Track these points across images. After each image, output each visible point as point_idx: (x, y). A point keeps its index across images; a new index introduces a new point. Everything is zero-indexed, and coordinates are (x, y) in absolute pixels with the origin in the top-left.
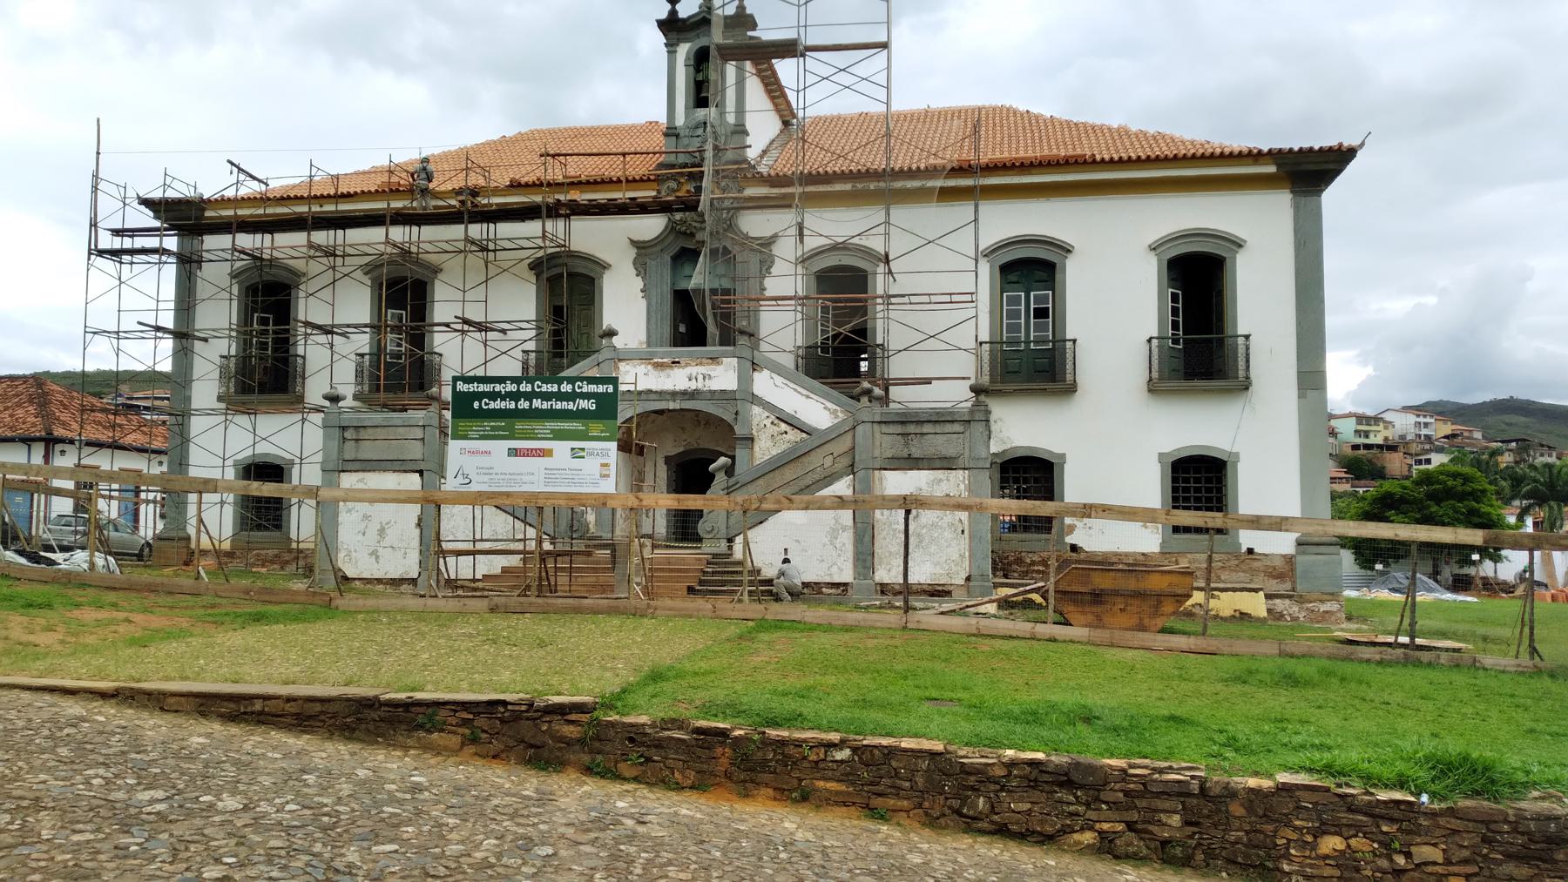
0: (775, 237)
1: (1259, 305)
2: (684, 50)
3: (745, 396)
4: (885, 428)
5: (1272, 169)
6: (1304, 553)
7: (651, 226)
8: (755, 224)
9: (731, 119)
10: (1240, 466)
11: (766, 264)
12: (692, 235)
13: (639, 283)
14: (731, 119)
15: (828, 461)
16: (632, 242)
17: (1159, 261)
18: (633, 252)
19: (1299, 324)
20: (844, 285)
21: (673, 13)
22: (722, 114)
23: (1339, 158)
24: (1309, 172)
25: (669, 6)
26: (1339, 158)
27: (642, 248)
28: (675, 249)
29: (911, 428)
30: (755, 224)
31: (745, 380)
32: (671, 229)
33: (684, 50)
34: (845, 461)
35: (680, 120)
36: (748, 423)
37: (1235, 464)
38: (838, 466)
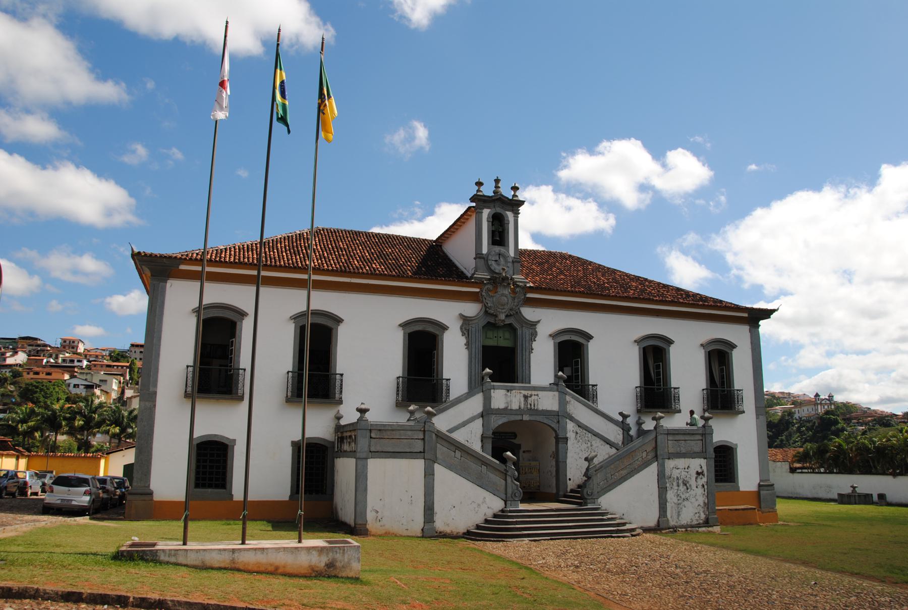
0: (539, 322)
3: (561, 415)
4: (670, 438)
5: (746, 315)
8: (529, 313)
9: (512, 253)
10: (738, 450)
11: (534, 335)
12: (496, 316)
13: (463, 340)
14: (512, 253)
15: (644, 454)
18: (460, 323)
20: (571, 352)
21: (478, 191)
23: (767, 314)
26: (767, 314)
27: (466, 322)
28: (485, 322)
29: (681, 437)
30: (529, 313)
31: (563, 403)
33: (486, 213)
38: (649, 457)
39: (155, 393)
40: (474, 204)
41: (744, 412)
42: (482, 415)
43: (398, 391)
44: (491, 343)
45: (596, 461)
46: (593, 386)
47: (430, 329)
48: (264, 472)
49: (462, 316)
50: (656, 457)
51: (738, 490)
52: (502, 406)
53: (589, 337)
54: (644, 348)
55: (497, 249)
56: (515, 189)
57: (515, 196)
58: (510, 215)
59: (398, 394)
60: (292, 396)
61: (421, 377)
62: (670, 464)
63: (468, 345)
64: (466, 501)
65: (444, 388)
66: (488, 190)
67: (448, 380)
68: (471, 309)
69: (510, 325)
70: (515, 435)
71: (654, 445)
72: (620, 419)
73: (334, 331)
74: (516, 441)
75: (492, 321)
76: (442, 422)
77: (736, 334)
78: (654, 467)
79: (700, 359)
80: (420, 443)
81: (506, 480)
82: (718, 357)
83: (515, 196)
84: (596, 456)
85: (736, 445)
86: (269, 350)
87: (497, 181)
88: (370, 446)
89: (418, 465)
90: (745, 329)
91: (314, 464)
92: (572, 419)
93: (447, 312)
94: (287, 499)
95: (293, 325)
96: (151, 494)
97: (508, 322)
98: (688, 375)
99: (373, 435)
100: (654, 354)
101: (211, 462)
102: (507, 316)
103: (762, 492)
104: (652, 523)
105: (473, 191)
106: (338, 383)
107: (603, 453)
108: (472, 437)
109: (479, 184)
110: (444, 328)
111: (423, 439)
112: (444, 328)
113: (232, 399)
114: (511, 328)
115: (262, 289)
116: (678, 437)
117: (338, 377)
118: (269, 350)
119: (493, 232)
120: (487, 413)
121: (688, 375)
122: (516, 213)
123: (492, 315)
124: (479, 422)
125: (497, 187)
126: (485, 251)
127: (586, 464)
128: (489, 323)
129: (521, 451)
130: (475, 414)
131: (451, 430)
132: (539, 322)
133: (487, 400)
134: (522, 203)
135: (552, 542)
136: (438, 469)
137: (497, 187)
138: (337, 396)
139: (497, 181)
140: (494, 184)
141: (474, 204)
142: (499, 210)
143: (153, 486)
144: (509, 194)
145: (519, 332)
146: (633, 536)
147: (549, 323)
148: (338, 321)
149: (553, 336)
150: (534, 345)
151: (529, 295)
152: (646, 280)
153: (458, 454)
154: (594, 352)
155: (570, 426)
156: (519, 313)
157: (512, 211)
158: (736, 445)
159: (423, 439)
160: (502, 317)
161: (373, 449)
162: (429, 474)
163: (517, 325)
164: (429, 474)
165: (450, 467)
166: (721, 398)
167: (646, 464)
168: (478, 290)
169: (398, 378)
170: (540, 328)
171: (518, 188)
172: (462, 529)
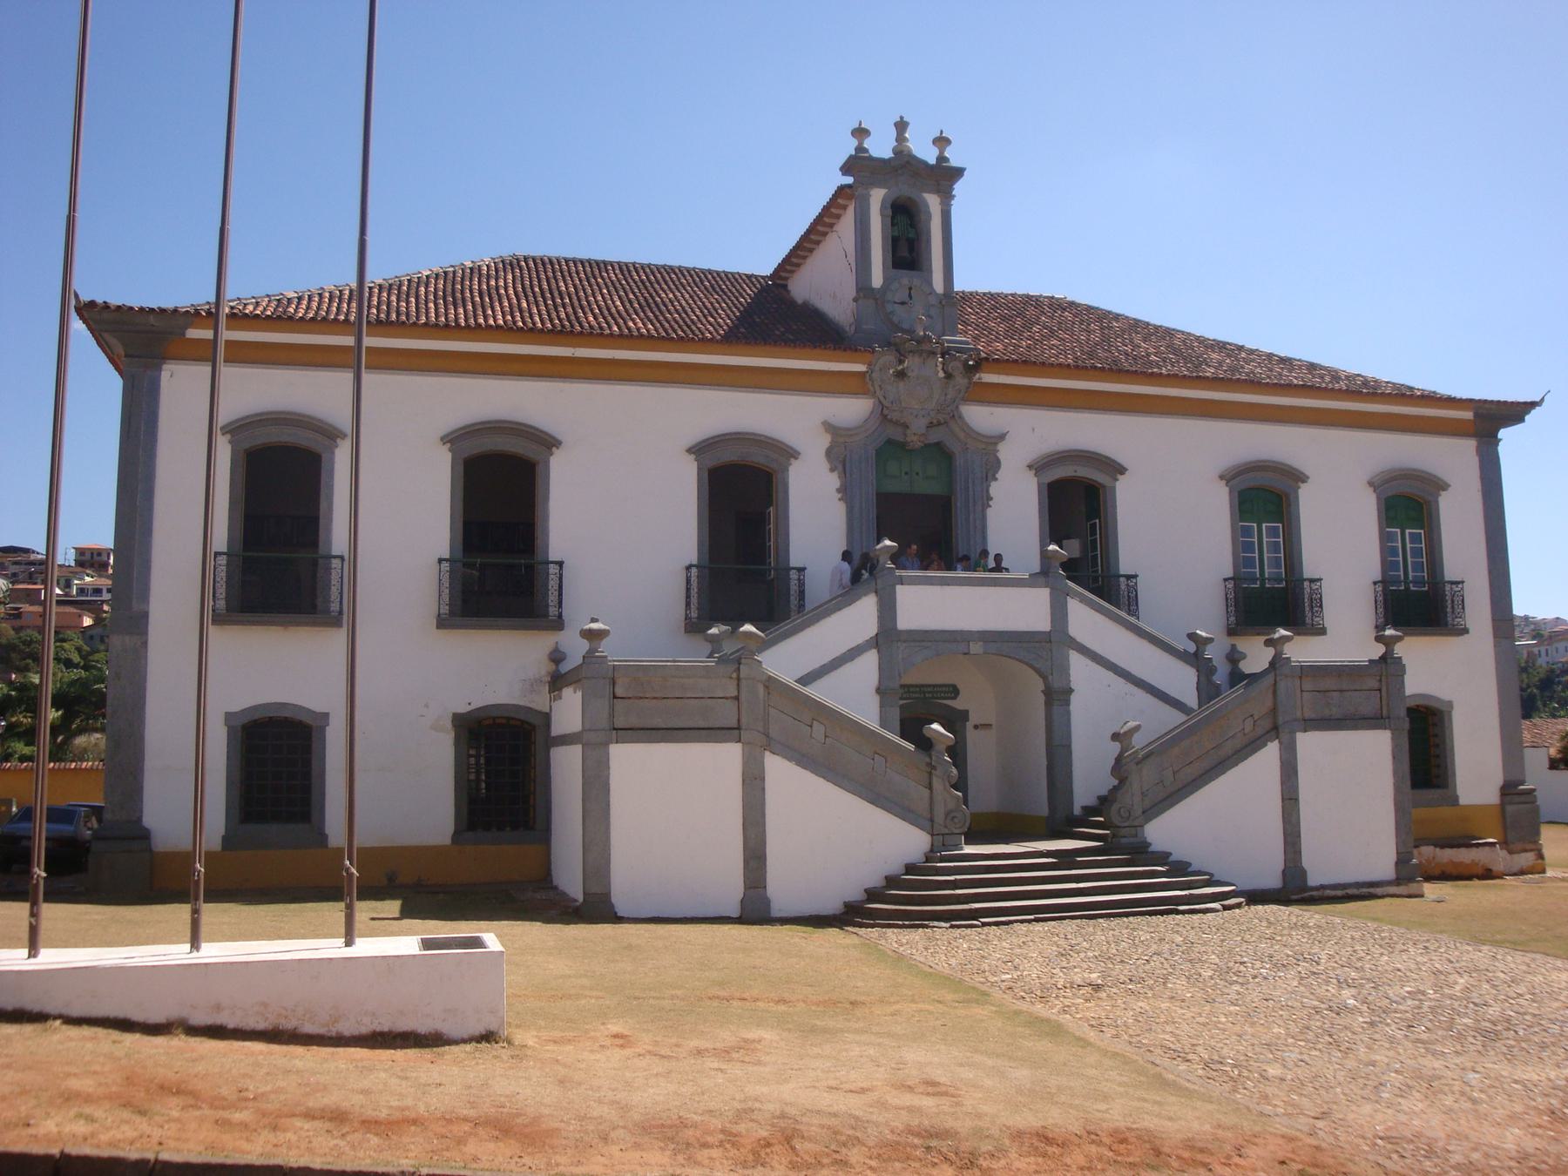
8: (980, 417)
9: (939, 287)
13: (833, 481)
14: (939, 287)
15: (1249, 725)
17: (1378, 498)
18: (825, 441)
19: (1490, 572)
20: (1078, 505)
22: (929, 282)
23: (1515, 412)
24: (1489, 420)
25: (855, 143)
26: (1515, 412)
30: (980, 417)
31: (1059, 613)
33: (877, 196)
35: (877, 280)
36: (1065, 670)
38: (1260, 731)
39: (145, 616)
40: (849, 180)
41: (1465, 631)
42: (875, 643)
43: (688, 597)
44: (893, 486)
45: (1138, 741)
46: (1129, 577)
47: (758, 458)
48: (396, 785)
49: (829, 427)
50: (1274, 731)
51: (1454, 801)
53: (1117, 469)
54: (1241, 493)
55: (906, 277)
56: (941, 141)
57: (942, 159)
58: (933, 201)
59: (688, 604)
60: (452, 613)
61: (741, 565)
62: (1309, 743)
63: (845, 491)
64: (838, 832)
65: (794, 587)
66: (881, 147)
67: (801, 570)
68: (852, 410)
69: (938, 444)
70: (954, 691)
71: (1269, 703)
72: (1192, 648)
73: (539, 469)
74: (958, 704)
75: (895, 433)
76: (787, 659)
77: (1450, 459)
78: (1271, 751)
79: (1366, 510)
80: (731, 706)
81: (930, 787)
82: (1407, 505)
83: (942, 159)
84: (1137, 728)
85: (1450, 704)
86: (395, 515)
87: (901, 126)
88: (612, 715)
89: (729, 755)
90: (1467, 447)
91: (502, 765)
93: (804, 423)
94: (447, 841)
95: (449, 456)
96: (145, 835)
97: (934, 437)
98: (1341, 548)
99: (619, 691)
100: (1264, 498)
101: (277, 763)
102: (931, 425)
103: (1509, 808)
104: (1271, 879)
105: (849, 147)
106: (553, 583)
107: (1155, 721)
108: (856, 694)
109: (860, 133)
110: (791, 454)
111: (737, 698)
112: (791, 454)
113: (314, 624)
114: (940, 454)
115: (367, 377)
117: (553, 569)
118: (395, 515)
120: (887, 637)
121: (1341, 548)
122: (947, 196)
123: (896, 423)
124: (871, 659)
125: (900, 138)
126: (877, 280)
127: (1115, 748)
128: (890, 442)
129: (969, 725)
130: (860, 641)
131: (806, 680)
132: (1002, 437)
133: (887, 610)
134: (958, 173)
135: (1038, 927)
137: (900, 138)
138: (553, 611)
139: (901, 126)
140: (893, 133)
141: (849, 180)
142: (904, 190)
143: (149, 820)
144: (929, 155)
145: (959, 462)
146: (1226, 908)
147: (1023, 437)
148: (549, 443)
149: (1038, 467)
150: (995, 489)
152: (1241, 348)
154: (1131, 507)
155: (1076, 661)
156: (956, 416)
157: (938, 191)
158: (1450, 704)
159: (737, 698)
160: (918, 425)
163: (955, 448)
167: (1252, 746)
168: (861, 368)
169: (688, 568)
170: (1004, 452)
171: (947, 141)
172: (832, 906)
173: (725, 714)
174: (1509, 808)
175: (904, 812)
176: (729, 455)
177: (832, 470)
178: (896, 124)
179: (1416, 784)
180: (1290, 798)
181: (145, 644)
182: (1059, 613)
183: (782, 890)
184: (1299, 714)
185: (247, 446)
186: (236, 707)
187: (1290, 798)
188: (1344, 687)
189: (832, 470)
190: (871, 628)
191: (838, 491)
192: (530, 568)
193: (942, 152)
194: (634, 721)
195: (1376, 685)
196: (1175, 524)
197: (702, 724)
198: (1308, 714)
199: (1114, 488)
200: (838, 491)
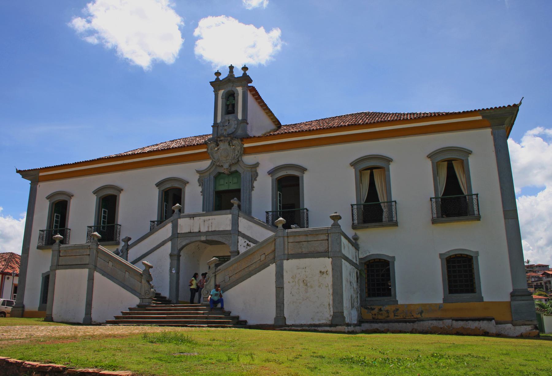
1: (480, 179)
2: (221, 92)
5: (480, 118)
6: (515, 300)
7: (205, 164)
9: (240, 117)
11: (255, 176)
12: (222, 166)
14: (240, 117)
15: (263, 257)
16: (198, 172)
18: (197, 176)
20: (289, 186)
21: (217, 79)
22: (236, 117)
25: (216, 77)
30: (249, 159)
31: (235, 223)
32: (213, 164)
33: (221, 92)
34: (271, 256)
35: (219, 120)
37: (477, 257)
42: (171, 239)
47: (177, 185)
51: (481, 299)
52: (187, 231)
53: (303, 170)
58: (240, 90)
62: (288, 264)
69: (236, 172)
78: (272, 268)
81: (141, 282)
83: (245, 74)
85: (477, 253)
92: (244, 236)
97: (233, 169)
102: (230, 166)
110: (186, 183)
114: (235, 173)
116: (298, 239)
119: (227, 106)
120: (175, 236)
124: (169, 244)
126: (219, 120)
130: (166, 238)
133: (175, 227)
136: (97, 275)
145: (242, 175)
149: (271, 173)
151: (246, 145)
153: (110, 264)
160: (226, 166)
161: (60, 264)
162: (91, 279)
163: (240, 170)
164: (91, 279)
165: (105, 274)
166: (454, 203)
167: (265, 266)
168: (205, 150)
170: (259, 170)
173: (86, 260)
174: (514, 303)
175: (133, 291)
176: (168, 186)
177: (200, 186)
178: (230, 67)
179: (451, 292)
180: (280, 288)
181: (28, 256)
182: (235, 223)
183: (94, 317)
184: (286, 252)
185: (52, 201)
186: (44, 272)
187: (280, 288)
188: (309, 240)
189: (200, 186)
190: (170, 234)
191: (201, 192)
192: (114, 226)
193: (245, 72)
194: (63, 263)
195: (326, 238)
196: (330, 188)
197: (80, 263)
198: (291, 252)
199: (303, 176)
200: (201, 192)
